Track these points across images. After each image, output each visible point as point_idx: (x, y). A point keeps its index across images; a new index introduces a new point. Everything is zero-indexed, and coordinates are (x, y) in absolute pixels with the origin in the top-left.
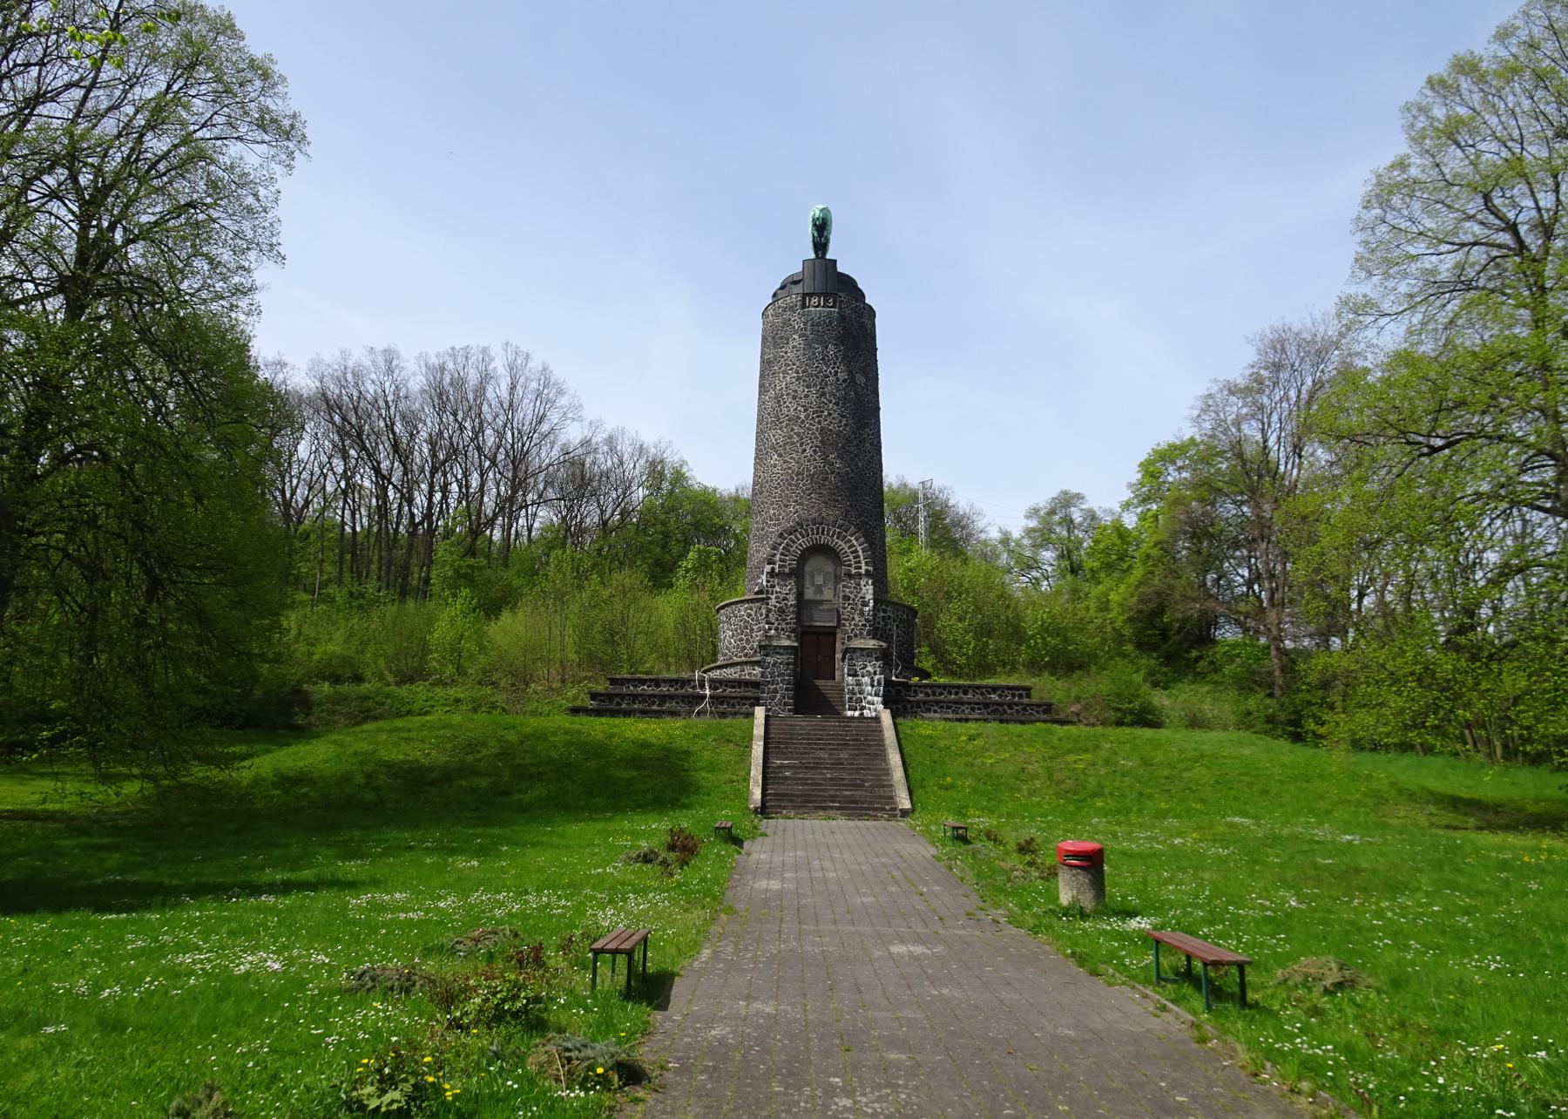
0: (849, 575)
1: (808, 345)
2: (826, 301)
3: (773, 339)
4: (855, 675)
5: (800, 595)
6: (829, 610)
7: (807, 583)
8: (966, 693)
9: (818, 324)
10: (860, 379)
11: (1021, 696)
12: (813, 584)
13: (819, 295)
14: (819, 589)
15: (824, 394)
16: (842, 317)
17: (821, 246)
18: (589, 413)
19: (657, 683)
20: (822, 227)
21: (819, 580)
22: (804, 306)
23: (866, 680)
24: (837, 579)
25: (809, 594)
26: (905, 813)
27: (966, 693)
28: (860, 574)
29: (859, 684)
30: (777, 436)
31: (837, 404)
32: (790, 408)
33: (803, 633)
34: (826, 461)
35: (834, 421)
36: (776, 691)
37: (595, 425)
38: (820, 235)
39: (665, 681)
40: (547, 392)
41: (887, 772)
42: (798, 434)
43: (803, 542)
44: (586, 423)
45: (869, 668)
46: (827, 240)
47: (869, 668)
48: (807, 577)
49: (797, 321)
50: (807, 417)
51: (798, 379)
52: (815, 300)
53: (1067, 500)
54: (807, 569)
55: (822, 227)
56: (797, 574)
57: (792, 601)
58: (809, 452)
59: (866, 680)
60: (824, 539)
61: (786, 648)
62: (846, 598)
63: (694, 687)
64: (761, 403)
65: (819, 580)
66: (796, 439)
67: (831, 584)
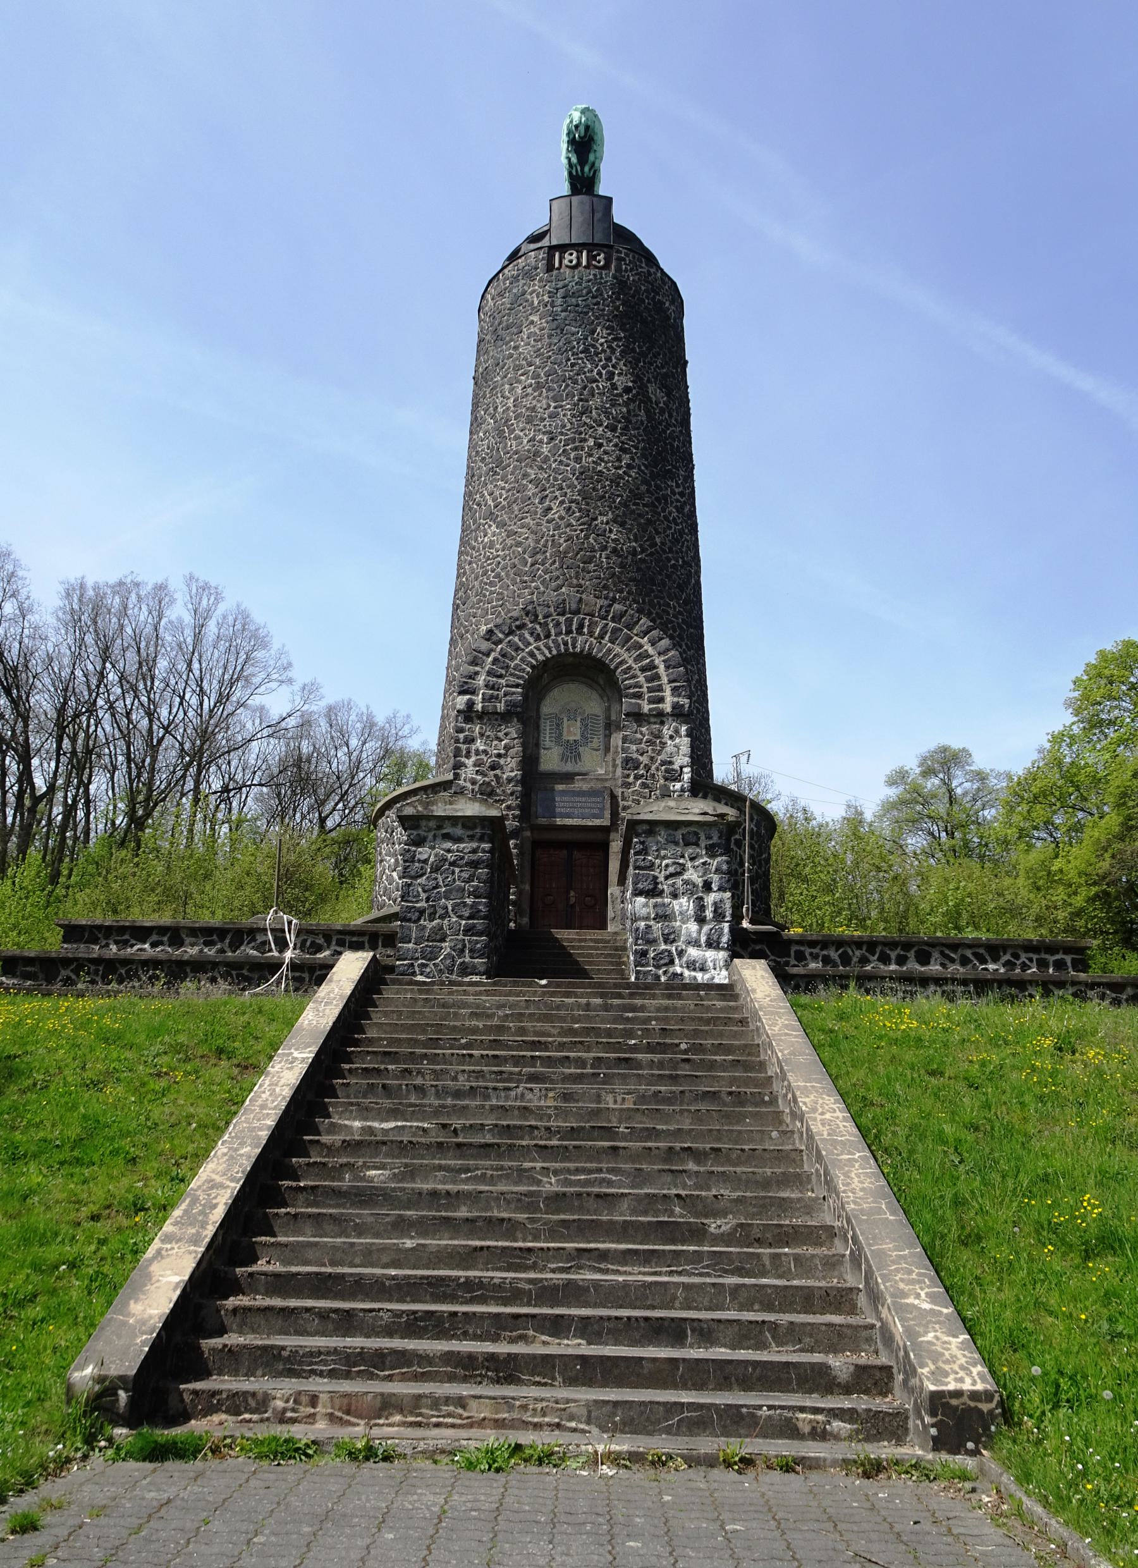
0: (638, 717)
2: (591, 258)
3: (495, 330)
4: (653, 892)
5: (529, 762)
6: (592, 793)
7: (547, 739)
8: (924, 959)
10: (655, 392)
11: (1060, 965)
12: (558, 739)
13: (578, 247)
14: (572, 751)
15: (586, 411)
16: (621, 284)
17: (583, 181)
18: (300, 676)
19: (174, 934)
20: (584, 143)
21: (573, 732)
22: (550, 268)
23: (684, 904)
24: (610, 727)
25: (551, 760)
26: (961, 1424)
27: (924, 959)
28: (660, 716)
29: (664, 916)
30: (497, 491)
31: (613, 429)
32: (522, 438)
33: (536, 844)
35: (606, 454)
36: (440, 936)
37: (309, 691)
38: (583, 160)
39: (194, 932)
40: (245, 640)
41: (791, 1166)
42: (536, 482)
43: (537, 650)
44: (297, 687)
45: (693, 875)
46: (596, 172)
47: (693, 875)
48: (547, 728)
49: (537, 292)
52: (570, 257)
53: (946, 761)
54: (547, 708)
55: (584, 143)
56: (525, 715)
57: (511, 769)
58: (557, 511)
59: (684, 904)
60: (582, 643)
61: (468, 822)
62: (630, 764)
64: (472, 446)
65: (573, 732)
66: (531, 489)
67: (597, 742)
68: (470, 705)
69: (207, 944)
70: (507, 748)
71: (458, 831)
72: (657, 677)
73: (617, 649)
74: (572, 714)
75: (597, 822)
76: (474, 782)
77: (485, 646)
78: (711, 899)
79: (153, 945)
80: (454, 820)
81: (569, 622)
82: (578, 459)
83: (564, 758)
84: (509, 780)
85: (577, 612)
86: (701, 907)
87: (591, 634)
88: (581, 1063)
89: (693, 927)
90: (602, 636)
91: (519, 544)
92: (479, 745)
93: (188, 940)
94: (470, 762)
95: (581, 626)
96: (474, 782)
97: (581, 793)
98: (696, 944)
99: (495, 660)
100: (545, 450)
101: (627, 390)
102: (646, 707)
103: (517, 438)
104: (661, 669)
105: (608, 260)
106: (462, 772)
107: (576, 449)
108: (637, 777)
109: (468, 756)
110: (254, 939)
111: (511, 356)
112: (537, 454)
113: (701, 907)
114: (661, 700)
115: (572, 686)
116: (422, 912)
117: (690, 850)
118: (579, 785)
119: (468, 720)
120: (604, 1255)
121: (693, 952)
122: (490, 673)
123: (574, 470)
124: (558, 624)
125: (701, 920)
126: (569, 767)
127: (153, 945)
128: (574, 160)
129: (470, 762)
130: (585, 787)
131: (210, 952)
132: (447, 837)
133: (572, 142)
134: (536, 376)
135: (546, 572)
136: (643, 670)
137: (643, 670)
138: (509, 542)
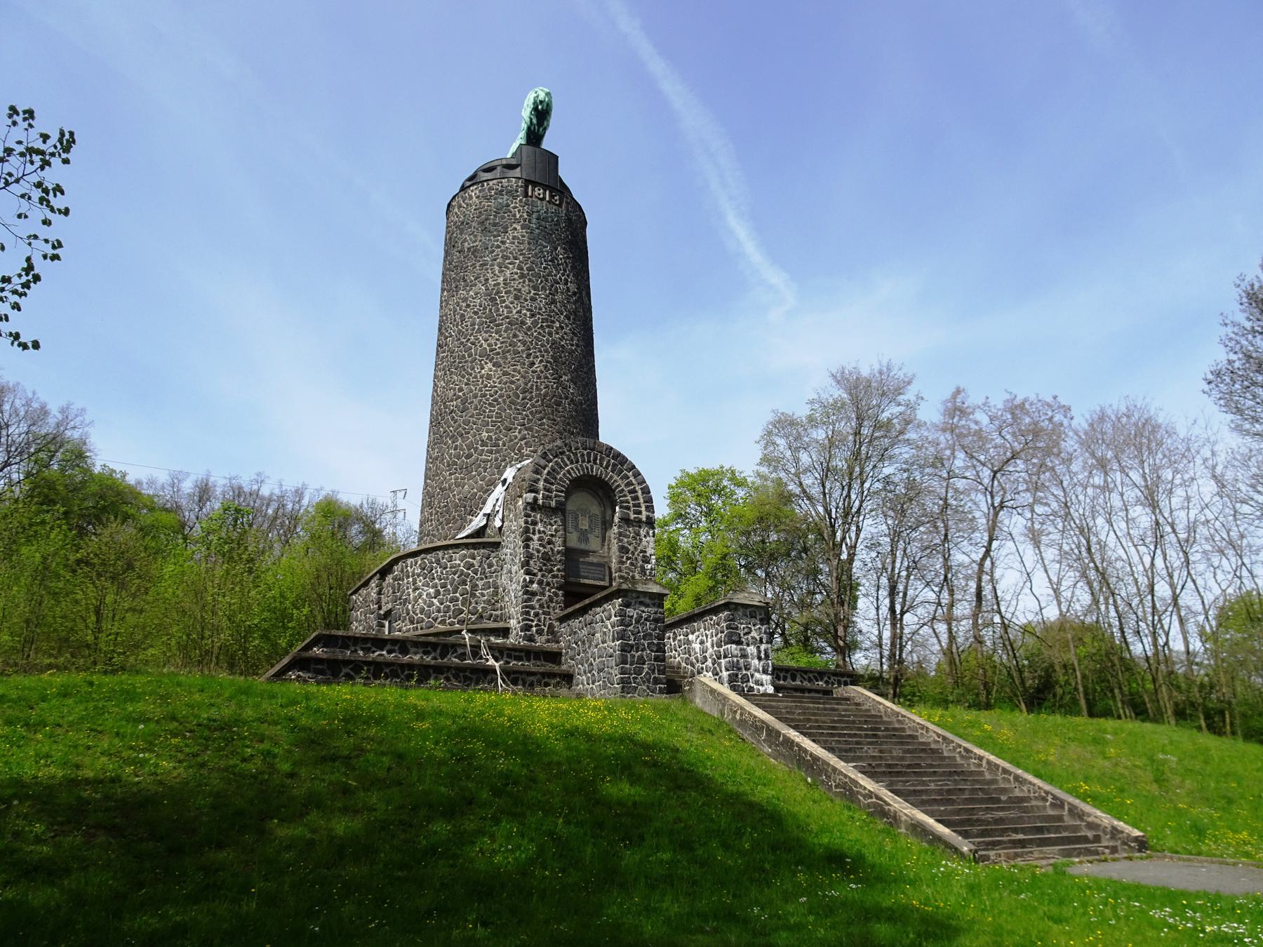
1: (534, 240)
4: (739, 643)
9: (545, 219)
12: (576, 527)
14: (584, 536)
15: (553, 302)
17: (534, 137)
20: (542, 113)
21: (584, 524)
28: (640, 521)
29: (744, 656)
34: (560, 384)
36: (642, 661)
42: (524, 343)
47: (754, 634)
50: (535, 323)
51: (522, 276)
55: (542, 113)
58: (538, 366)
59: (752, 650)
60: (596, 470)
63: (462, 656)
65: (584, 524)
67: (598, 532)
68: (535, 499)
69: (426, 653)
70: (556, 531)
71: (647, 601)
72: (636, 498)
73: (615, 477)
74: (585, 512)
75: (602, 583)
76: (538, 551)
77: (543, 462)
78: (763, 647)
79: (389, 652)
80: (645, 594)
81: (589, 454)
82: (550, 334)
83: (580, 540)
84: (559, 552)
85: (593, 449)
86: (759, 652)
87: (601, 465)
88: (860, 736)
89: (756, 661)
90: (607, 467)
91: (512, 382)
92: (540, 527)
93: (412, 650)
94: (536, 537)
95: (595, 459)
96: (538, 551)
97: (592, 564)
98: (757, 670)
99: (549, 473)
100: (529, 321)
101: (575, 294)
102: (632, 516)
103: (507, 307)
104: (640, 492)
105: (561, 200)
106: (531, 543)
107: (548, 326)
108: (628, 558)
109: (534, 533)
110: (456, 651)
111: (498, 247)
112: (523, 323)
113: (759, 652)
114: (640, 513)
115: (584, 494)
116: (632, 646)
117: (753, 620)
118: (591, 559)
119: (533, 509)
120: (992, 809)
121: (757, 675)
122: (546, 481)
123: (548, 341)
124: (583, 455)
125: (760, 659)
126: (583, 546)
127: (389, 652)
128: (535, 121)
129: (536, 537)
130: (595, 560)
131: (428, 659)
132: (642, 603)
133: (535, 109)
134: (520, 268)
135: (533, 406)
136: (630, 492)
137: (630, 492)
138: (504, 379)
